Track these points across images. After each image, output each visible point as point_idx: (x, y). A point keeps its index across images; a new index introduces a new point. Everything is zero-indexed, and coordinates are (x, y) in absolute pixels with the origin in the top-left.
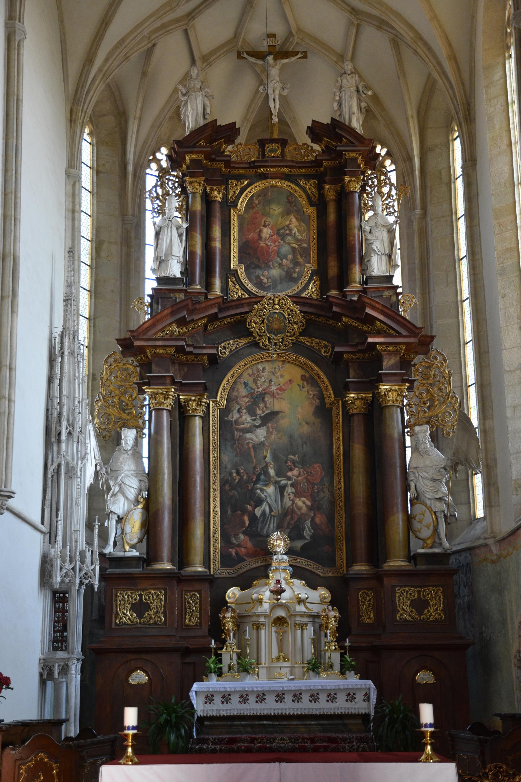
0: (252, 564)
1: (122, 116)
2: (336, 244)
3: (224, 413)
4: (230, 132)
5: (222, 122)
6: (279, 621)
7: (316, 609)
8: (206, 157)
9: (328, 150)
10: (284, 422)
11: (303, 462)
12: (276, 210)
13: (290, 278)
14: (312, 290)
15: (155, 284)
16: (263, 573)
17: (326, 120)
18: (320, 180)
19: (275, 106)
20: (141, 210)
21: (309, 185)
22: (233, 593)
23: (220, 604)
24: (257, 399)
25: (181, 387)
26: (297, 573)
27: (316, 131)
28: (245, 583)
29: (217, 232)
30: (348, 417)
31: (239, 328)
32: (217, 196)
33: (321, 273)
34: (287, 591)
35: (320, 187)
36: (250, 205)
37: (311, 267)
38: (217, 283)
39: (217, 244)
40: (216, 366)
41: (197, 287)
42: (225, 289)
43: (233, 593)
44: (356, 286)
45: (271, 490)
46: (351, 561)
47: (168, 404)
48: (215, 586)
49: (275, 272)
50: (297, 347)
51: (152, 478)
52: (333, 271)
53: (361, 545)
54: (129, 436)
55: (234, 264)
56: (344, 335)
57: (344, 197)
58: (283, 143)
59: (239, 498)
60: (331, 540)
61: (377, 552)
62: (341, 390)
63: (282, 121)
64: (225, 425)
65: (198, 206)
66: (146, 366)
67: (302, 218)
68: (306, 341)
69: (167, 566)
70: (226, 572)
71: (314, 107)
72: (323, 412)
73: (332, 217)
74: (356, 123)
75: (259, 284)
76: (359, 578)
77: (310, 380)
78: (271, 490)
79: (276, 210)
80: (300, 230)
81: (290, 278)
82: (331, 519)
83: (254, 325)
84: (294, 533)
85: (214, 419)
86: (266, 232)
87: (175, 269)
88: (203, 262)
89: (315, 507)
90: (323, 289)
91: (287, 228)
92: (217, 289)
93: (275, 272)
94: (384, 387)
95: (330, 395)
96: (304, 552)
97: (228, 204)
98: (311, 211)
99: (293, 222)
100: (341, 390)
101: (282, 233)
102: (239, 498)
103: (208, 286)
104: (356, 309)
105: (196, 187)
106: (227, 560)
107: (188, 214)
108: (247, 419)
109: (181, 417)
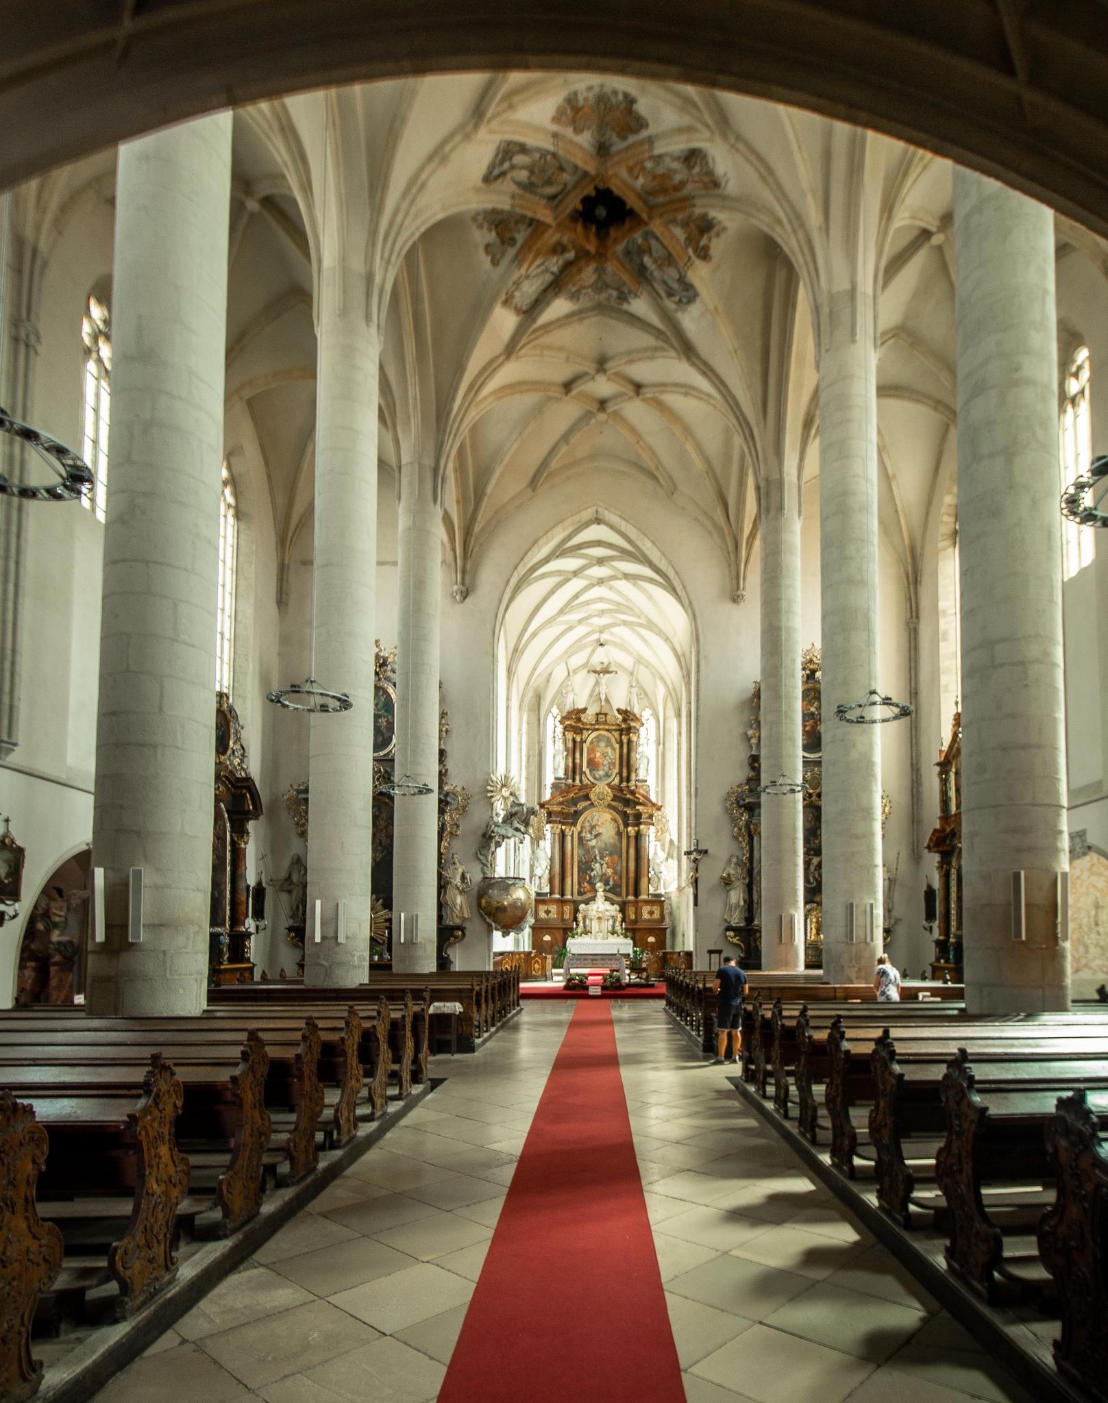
0: (589, 895)
1: (539, 698)
2: (626, 764)
3: (580, 833)
4: (584, 710)
5: (581, 706)
6: (599, 918)
7: (614, 913)
8: (574, 722)
9: (625, 720)
10: (604, 837)
11: (611, 854)
12: (602, 744)
13: (607, 775)
14: (617, 781)
15: (553, 780)
16: (593, 899)
17: (623, 708)
18: (621, 731)
19: (603, 698)
20: (544, 742)
21: (617, 734)
22: (582, 907)
23: (576, 911)
24: (593, 827)
25: (563, 824)
26: (607, 899)
27: (618, 710)
28: (587, 903)
29: (578, 755)
30: (628, 837)
31: (587, 797)
32: (578, 739)
33: (620, 773)
34: (601, 908)
35: (621, 735)
36: (592, 742)
37: (616, 770)
38: (578, 778)
39: (578, 761)
40: (577, 814)
41: (570, 781)
42: (581, 781)
43: (582, 907)
44: (632, 783)
45: (598, 865)
46: (627, 895)
47: (558, 831)
48: (575, 904)
49: (601, 773)
50: (610, 806)
51: (552, 859)
52: (625, 774)
53: (631, 889)
54: (541, 842)
55: (585, 768)
56: (627, 803)
57: (629, 741)
58: (606, 715)
59: (585, 868)
60: (620, 886)
61: (637, 894)
62: (626, 825)
63: (607, 700)
64: (581, 839)
65: (570, 745)
66: (550, 814)
67: (614, 749)
68: (613, 803)
69: (557, 896)
70: (580, 898)
71: (619, 702)
72: (619, 834)
73: (625, 750)
74: (636, 711)
75: (595, 778)
76: (630, 902)
77: (615, 820)
78: (598, 865)
79: (602, 744)
80: (613, 755)
81: (607, 775)
82: (621, 878)
83: (592, 796)
84: (606, 884)
85: (576, 836)
86: (598, 755)
87: (561, 774)
88: (573, 770)
89: (615, 873)
90: (621, 781)
91: (608, 754)
92: (577, 782)
93: (601, 773)
94: (642, 827)
95: (622, 827)
96: (609, 891)
97: (582, 742)
98: (617, 746)
99: (609, 750)
100: (626, 825)
101: (605, 755)
102: (585, 868)
103: (574, 780)
104: (633, 793)
105: (570, 735)
106: (580, 893)
107: (567, 749)
108: (589, 836)
109: (563, 835)
